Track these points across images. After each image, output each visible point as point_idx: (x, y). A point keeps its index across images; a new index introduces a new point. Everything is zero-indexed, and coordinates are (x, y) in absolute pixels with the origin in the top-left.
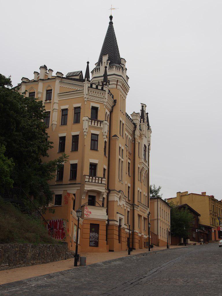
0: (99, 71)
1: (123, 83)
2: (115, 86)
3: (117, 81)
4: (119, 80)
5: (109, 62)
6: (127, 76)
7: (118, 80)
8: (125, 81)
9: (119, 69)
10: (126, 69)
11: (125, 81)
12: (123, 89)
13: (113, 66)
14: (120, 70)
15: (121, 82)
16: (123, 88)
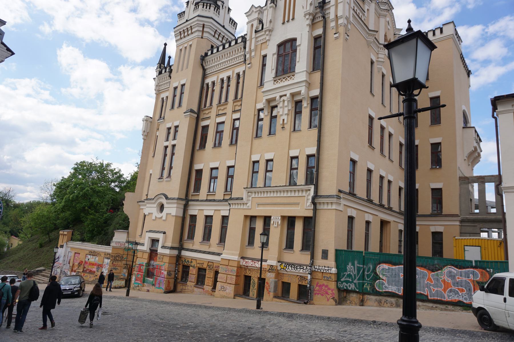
0: (183, 16)
1: (216, 29)
2: (200, 34)
3: (202, 25)
4: (205, 24)
6: (230, 19)
7: (204, 25)
8: (223, 27)
9: (208, 7)
10: (229, 9)
11: (223, 27)
12: (218, 39)
13: (198, 4)
14: (210, 9)
15: (210, 28)
16: (217, 36)
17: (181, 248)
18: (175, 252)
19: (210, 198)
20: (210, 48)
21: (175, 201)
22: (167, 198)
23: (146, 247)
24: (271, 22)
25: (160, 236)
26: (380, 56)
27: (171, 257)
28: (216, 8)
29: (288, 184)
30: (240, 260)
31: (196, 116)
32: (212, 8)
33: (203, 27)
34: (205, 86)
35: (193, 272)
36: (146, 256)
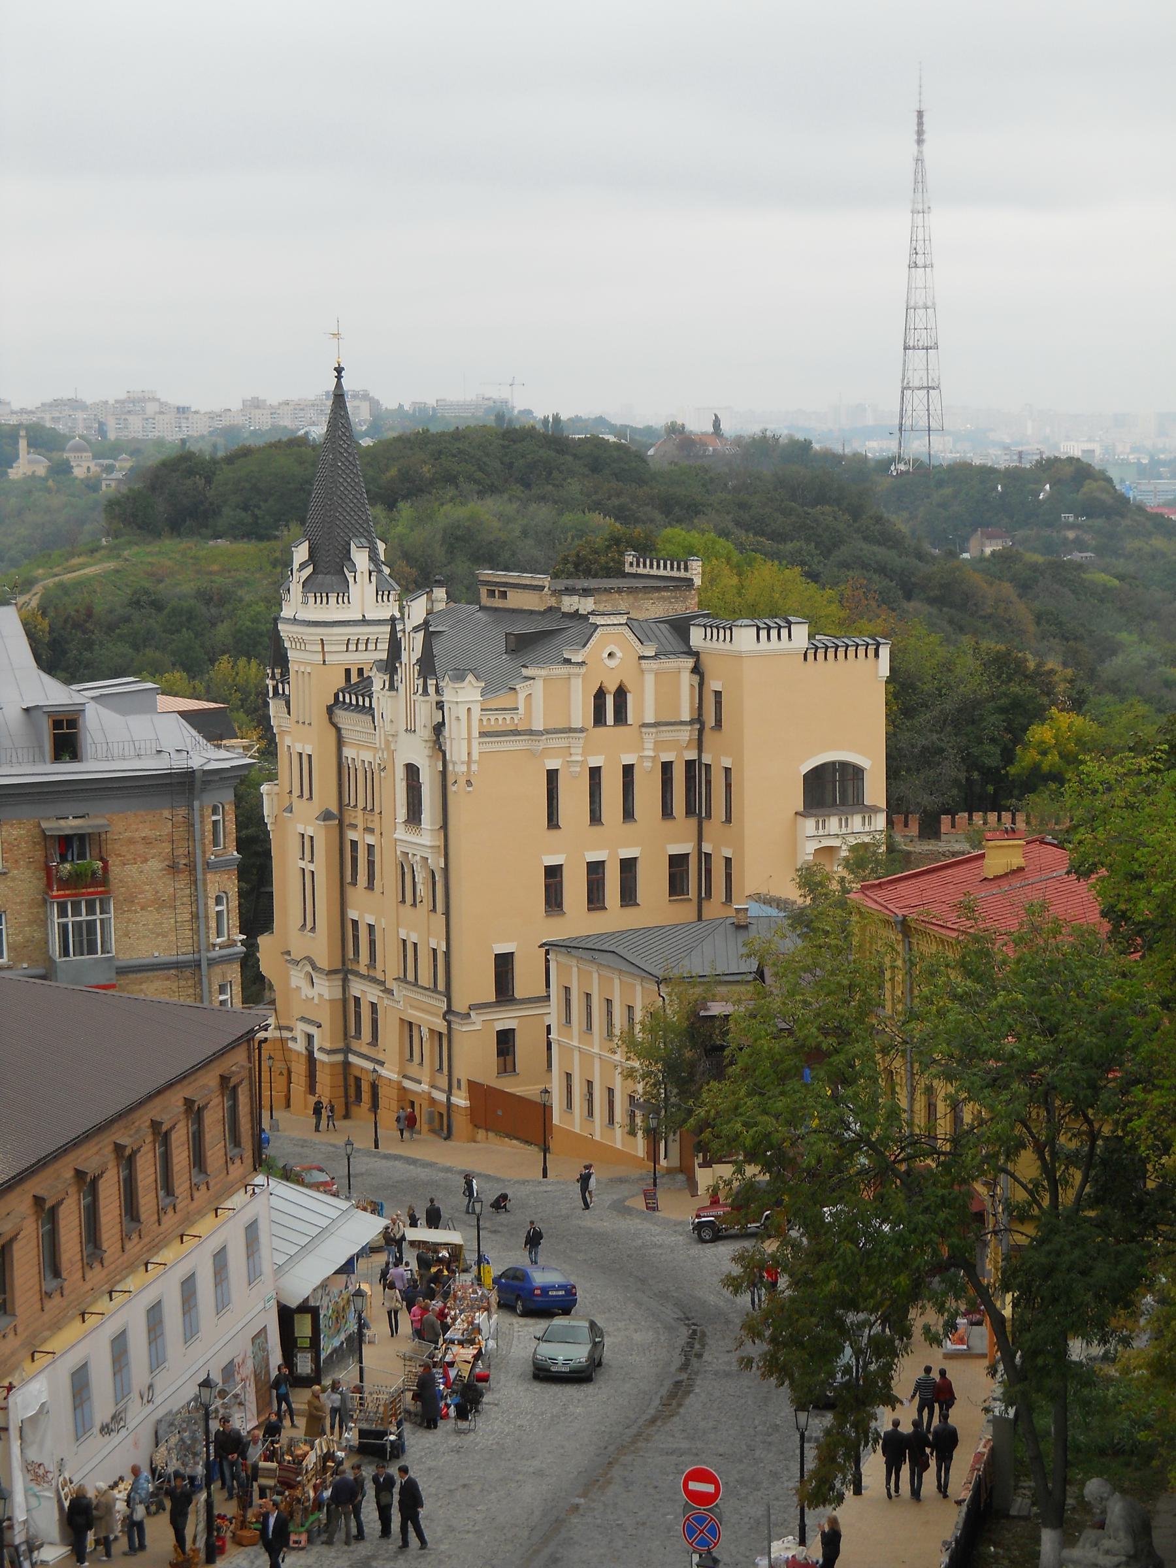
5: (310, 569)
7: (322, 640)
8: (364, 622)
9: (325, 599)
14: (327, 603)
16: (352, 647)
17: (347, 1050)
18: (339, 1058)
19: (372, 974)
20: (342, 684)
21: (325, 977)
22: (314, 967)
23: (299, 1046)
24: (392, 721)
25: (312, 1030)
26: (573, 751)
27: (333, 1065)
28: (341, 594)
29: (432, 986)
30: (401, 1079)
31: (337, 822)
32: (333, 600)
33: (323, 645)
34: (344, 760)
35: (365, 1087)
36: (303, 1060)
